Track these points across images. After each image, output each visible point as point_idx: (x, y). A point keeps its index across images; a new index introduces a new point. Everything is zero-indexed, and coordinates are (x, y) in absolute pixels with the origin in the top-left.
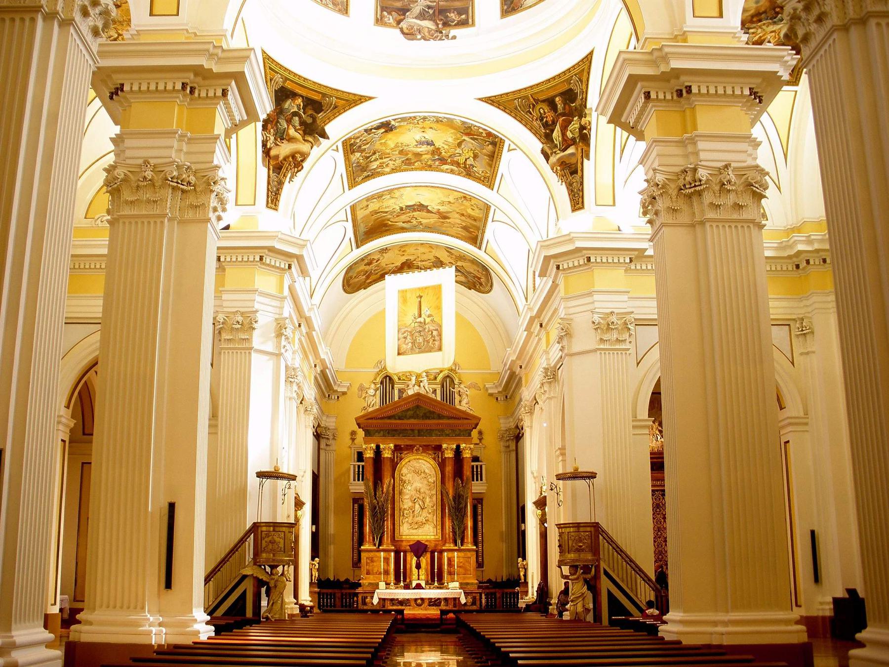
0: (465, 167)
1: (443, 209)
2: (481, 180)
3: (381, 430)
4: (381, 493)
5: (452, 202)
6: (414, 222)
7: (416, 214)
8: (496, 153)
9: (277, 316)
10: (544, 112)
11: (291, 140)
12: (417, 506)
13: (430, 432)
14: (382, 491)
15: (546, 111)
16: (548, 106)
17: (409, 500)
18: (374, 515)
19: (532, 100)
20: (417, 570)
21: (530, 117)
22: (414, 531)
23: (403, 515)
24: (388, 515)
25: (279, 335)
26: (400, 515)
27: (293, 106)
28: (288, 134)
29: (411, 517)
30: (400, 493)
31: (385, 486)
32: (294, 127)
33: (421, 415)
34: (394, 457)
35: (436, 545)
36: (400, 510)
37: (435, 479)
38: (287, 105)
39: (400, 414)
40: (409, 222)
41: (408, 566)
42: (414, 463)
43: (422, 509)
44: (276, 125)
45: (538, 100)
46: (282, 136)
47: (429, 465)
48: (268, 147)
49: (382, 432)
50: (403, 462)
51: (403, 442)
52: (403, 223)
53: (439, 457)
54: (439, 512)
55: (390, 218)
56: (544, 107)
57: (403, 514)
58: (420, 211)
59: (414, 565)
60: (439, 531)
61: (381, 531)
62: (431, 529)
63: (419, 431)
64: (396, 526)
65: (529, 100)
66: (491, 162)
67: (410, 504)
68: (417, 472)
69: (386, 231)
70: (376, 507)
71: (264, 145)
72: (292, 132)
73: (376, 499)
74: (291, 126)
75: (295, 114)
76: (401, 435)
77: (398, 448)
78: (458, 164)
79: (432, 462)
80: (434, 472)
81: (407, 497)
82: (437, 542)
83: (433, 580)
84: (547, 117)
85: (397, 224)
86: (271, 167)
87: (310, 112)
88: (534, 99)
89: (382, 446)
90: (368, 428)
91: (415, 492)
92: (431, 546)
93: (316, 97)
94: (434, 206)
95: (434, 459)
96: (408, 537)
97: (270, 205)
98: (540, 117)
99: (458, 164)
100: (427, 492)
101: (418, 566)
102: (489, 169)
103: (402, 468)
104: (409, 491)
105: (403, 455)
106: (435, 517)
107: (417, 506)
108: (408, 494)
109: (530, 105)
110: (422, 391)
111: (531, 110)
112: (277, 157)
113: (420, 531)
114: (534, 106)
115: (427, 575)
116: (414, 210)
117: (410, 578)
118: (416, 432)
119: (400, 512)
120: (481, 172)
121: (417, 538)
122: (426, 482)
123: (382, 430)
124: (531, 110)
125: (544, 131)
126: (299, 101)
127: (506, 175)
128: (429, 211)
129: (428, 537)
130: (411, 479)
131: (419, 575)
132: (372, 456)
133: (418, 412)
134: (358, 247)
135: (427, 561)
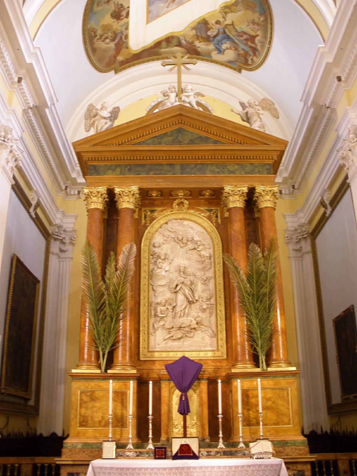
3: (117, 166)
17: (166, 289)
22: (176, 343)
23: (156, 315)
29: (169, 319)
30: (151, 275)
35: (217, 370)
37: (211, 251)
41: (164, 409)
42: (174, 225)
43: (190, 303)
47: (200, 229)
49: (118, 170)
50: (156, 224)
53: (217, 217)
54: (222, 308)
57: (156, 312)
60: (223, 343)
62: (208, 340)
67: (169, 295)
68: (180, 241)
79: (207, 224)
80: (209, 241)
81: (163, 282)
82: (219, 364)
83: (214, 435)
89: (117, 190)
91: (176, 274)
92: (208, 369)
95: (209, 218)
96: (164, 354)
100: (199, 274)
101: (184, 410)
105: (156, 214)
106: (213, 318)
107: (180, 297)
108: (163, 277)
113: (187, 343)
115: (202, 426)
117: (167, 433)
119: (149, 310)
123: (119, 166)
129: (202, 354)
130: (169, 252)
131: (185, 427)
132: (100, 206)
135: (200, 398)
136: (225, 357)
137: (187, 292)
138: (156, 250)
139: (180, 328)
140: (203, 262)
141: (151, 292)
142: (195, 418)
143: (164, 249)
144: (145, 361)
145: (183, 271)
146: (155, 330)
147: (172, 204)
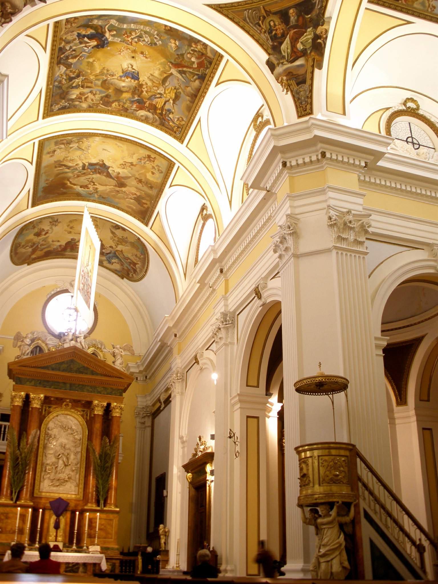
0: (161, 114)
1: (123, 172)
2: (173, 130)
4: (25, 444)
5: (134, 164)
6: (91, 187)
7: (96, 176)
8: (201, 90)
10: (275, 25)
12: (61, 462)
13: (82, 387)
14: (27, 442)
15: (277, 23)
16: (280, 18)
17: (52, 456)
18: (15, 466)
19: (263, 11)
20: (55, 530)
21: (258, 29)
22: (55, 488)
23: (45, 471)
24: (29, 468)
26: (41, 471)
29: (53, 474)
30: (45, 447)
31: (30, 438)
33: (75, 369)
34: (42, 409)
36: (42, 464)
39: (54, 366)
40: (86, 187)
42: (61, 418)
43: (66, 466)
45: (270, 12)
50: (51, 416)
51: (54, 394)
52: (81, 187)
55: (70, 178)
56: (275, 19)
58: (99, 173)
59: (52, 525)
61: (21, 485)
63: (71, 385)
64: (36, 482)
65: (259, 10)
66: (191, 104)
67: (54, 460)
68: (64, 428)
69: (64, 193)
70: (18, 458)
73: (19, 449)
76: (53, 387)
77: (47, 401)
78: (153, 108)
81: (51, 452)
82: (78, 502)
83: (71, 542)
84: (276, 30)
85: (75, 187)
88: (266, 11)
90: (20, 376)
94: (115, 169)
96: (48, 494)
98: (270, 29)
99: (153, 108)
100: (73, 449)
102: (187, 113)
103: (49, 422)
104: (54, 445)
105: (51, 409)
107: (61, 462)
109: (260, 17)
110: (78, 345)
111: (260, 22)
113: (61, 488)
114: (264, 18)
115: (65, 537)
116: (95, 172)
118: (68, 385)
119: (42, 468)
120: (176, 120)
121: (57, 496)
122: (71, 439)
124: (260, 22)
125: (271, 44)
127: (203, 122)
128: (109, 175)
129: (69, 496)
130: (57, 434)
133: (72, 366)
134: (33, 205)
136: (82, 498)
137: (65, 459)
138: (50, 432)
139: (59, 480)
140: (75, 442)
141: (44, 457)
142: (62, 531)
143: (55, 432)
144: (36, 497)
145: (63, 446)
146: (44, 479)
147: (62, 404)
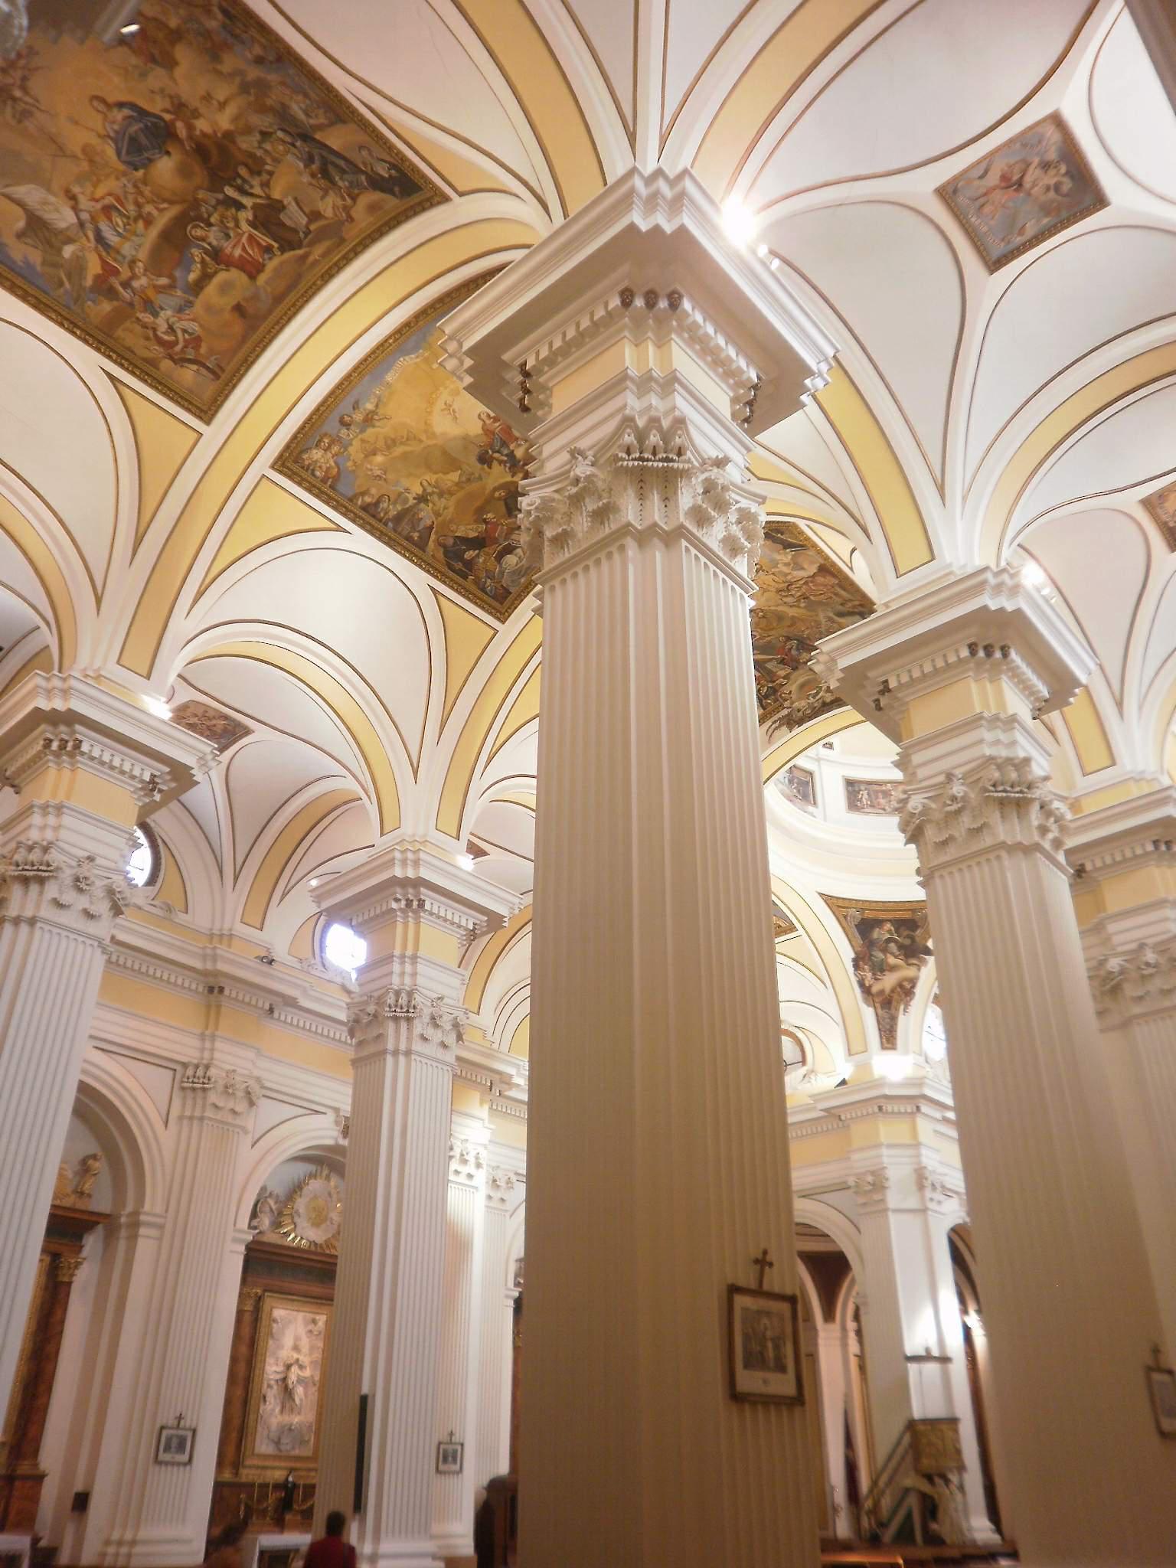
9: (916, 1167)
11: (893, 968)
25: (921, 1187)
27: (881, 934)
28: (888, 964)
32: (892, 954)
38: (876, 934)
44: (870, 960)
46: (880, 969)
48: (867, 985)
71: (861, 984)
72: (892, 960)
74: (888, 955)
75: (889, 941)
86: (878, 1005)
87: (906, 933)
93: (907, 915)
97: (886, 1045)
112: (882, 992)
126: (888, 926)
